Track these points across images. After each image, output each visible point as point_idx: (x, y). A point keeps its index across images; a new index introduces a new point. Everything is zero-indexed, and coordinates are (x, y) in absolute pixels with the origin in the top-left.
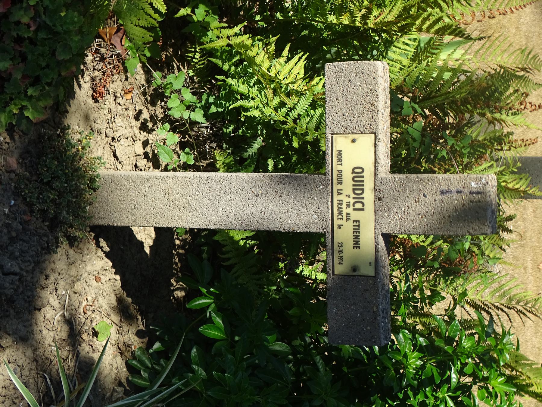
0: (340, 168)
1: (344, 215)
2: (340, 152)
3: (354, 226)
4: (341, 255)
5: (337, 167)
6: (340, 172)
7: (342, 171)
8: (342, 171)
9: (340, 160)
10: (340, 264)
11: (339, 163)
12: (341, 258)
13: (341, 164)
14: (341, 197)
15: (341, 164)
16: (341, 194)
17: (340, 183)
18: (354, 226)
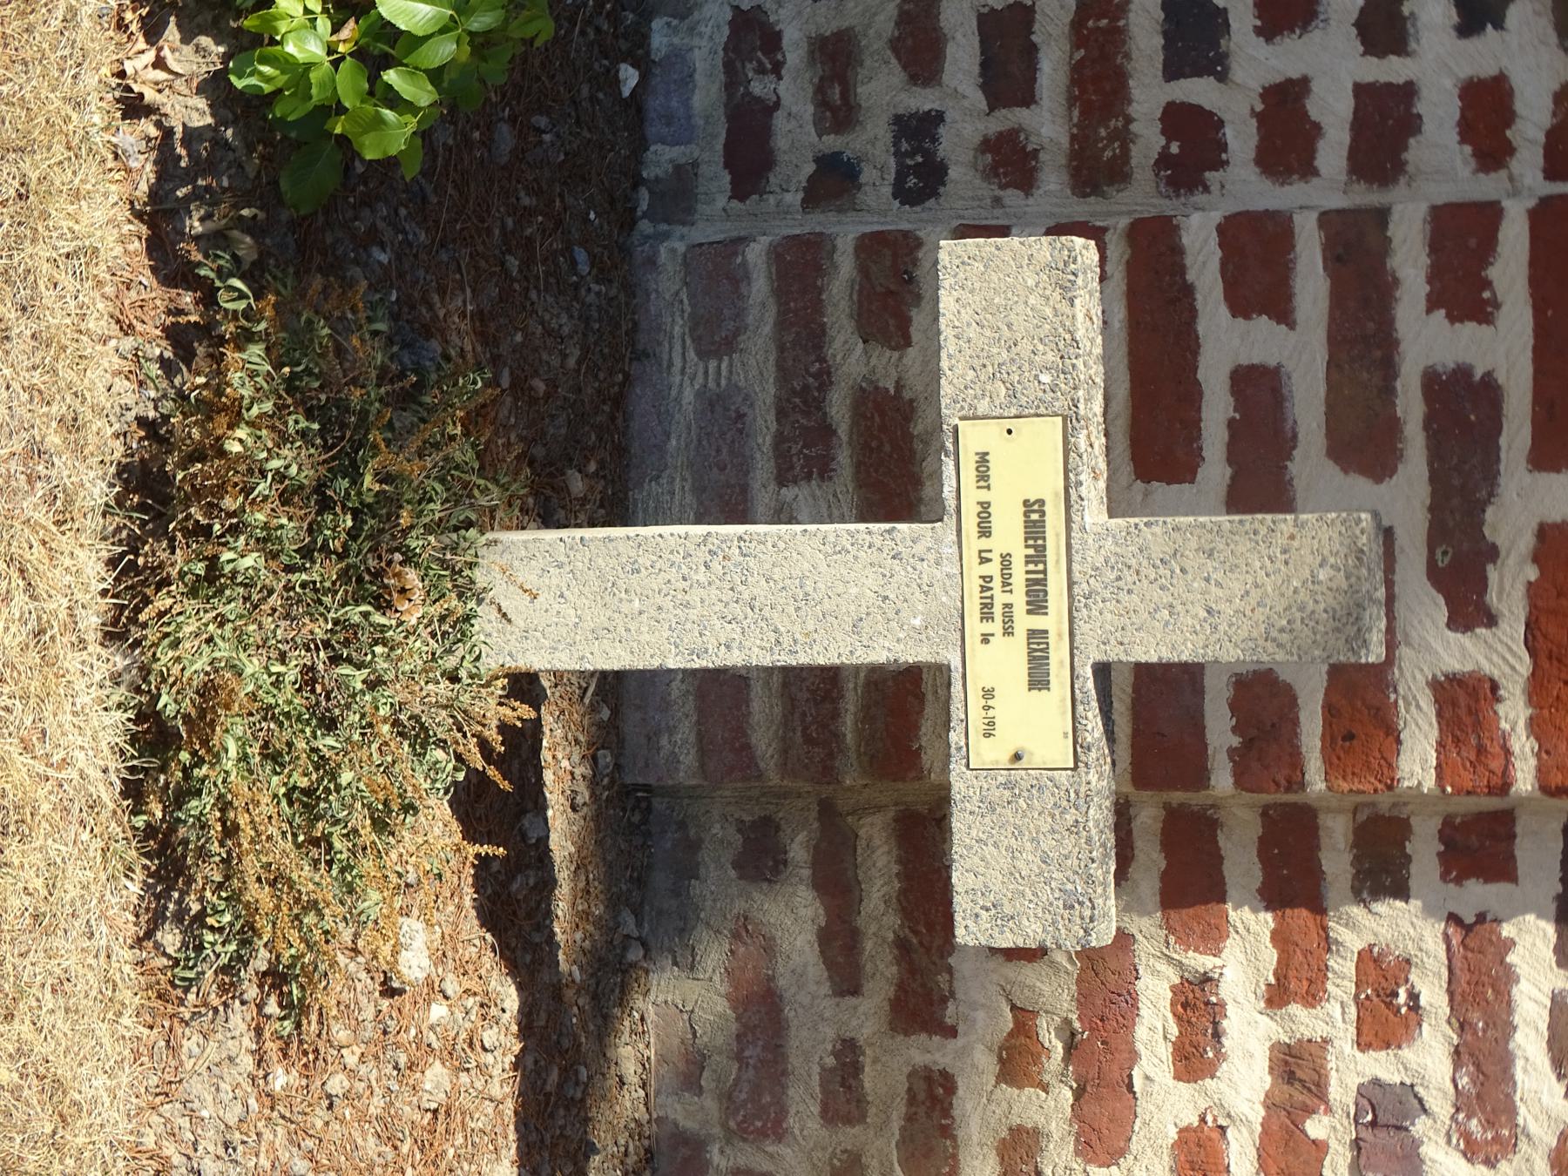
0: (984, 495)
1: (998, 610)
2: (983, 459)
3: (1028, 572)
4: (991, 713)
5: (972, 496)
6: (985, 506)
7: (989, 504)
8: (989, 504)
9: (983, 477)
10: (988, 735)
11: (982, 483)
12: (991, 723)
13: (988, 487)
14: (987, 569)
15: (988, 487)
16: (989, 560)
17: (985, 532)
18: (1028, 572)
